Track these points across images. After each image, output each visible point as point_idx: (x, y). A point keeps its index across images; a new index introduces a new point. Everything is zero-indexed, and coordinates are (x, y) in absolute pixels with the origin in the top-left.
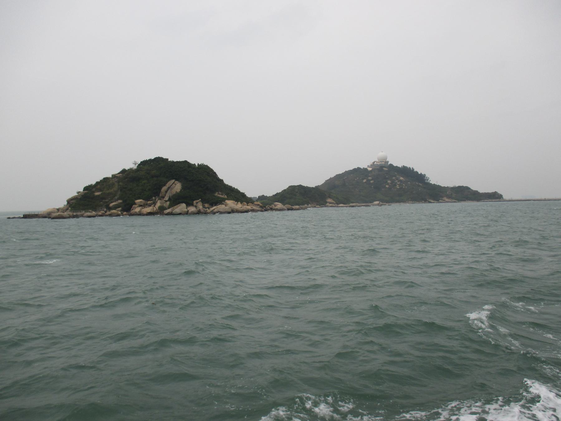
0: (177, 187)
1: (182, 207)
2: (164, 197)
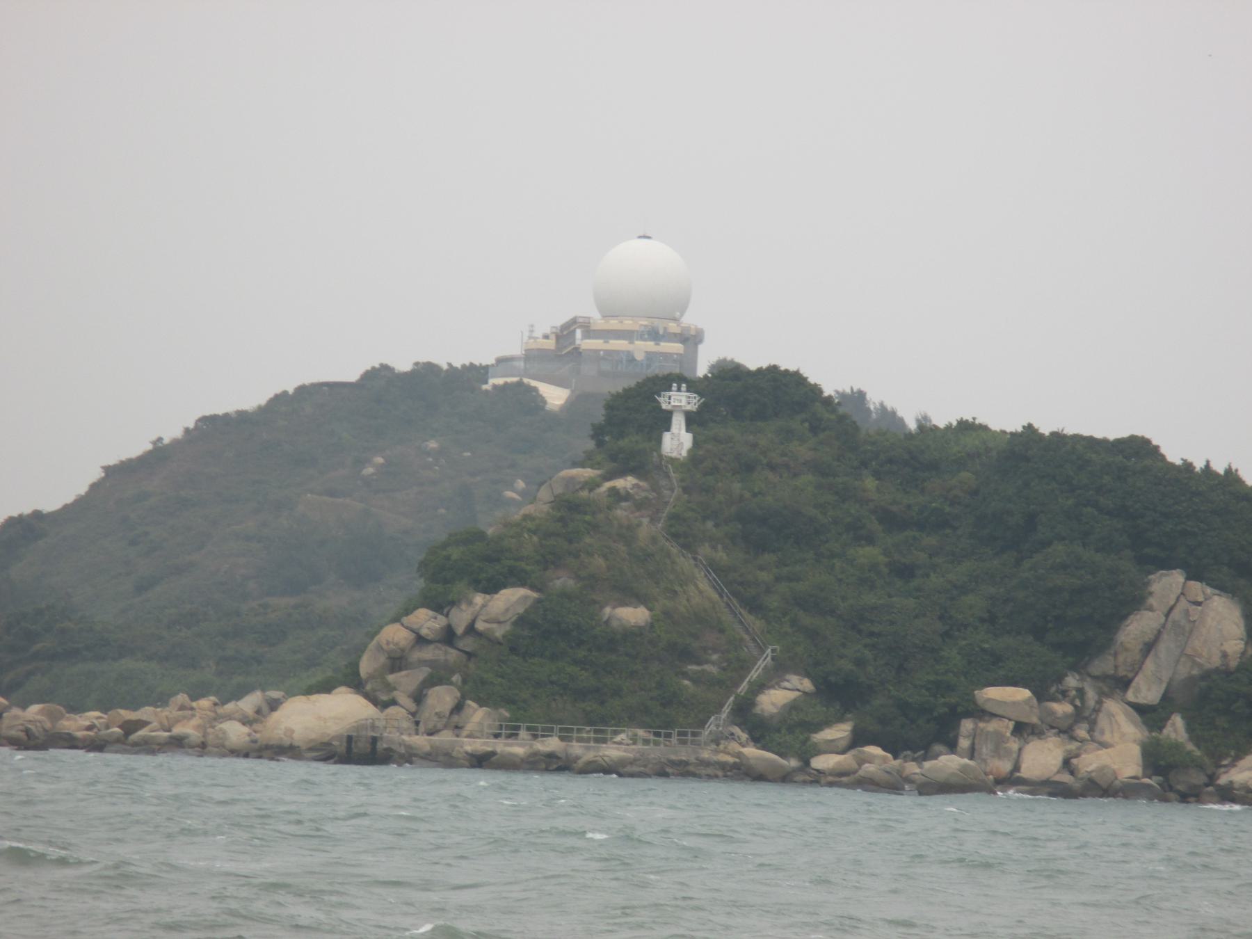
2: (1124, 684)
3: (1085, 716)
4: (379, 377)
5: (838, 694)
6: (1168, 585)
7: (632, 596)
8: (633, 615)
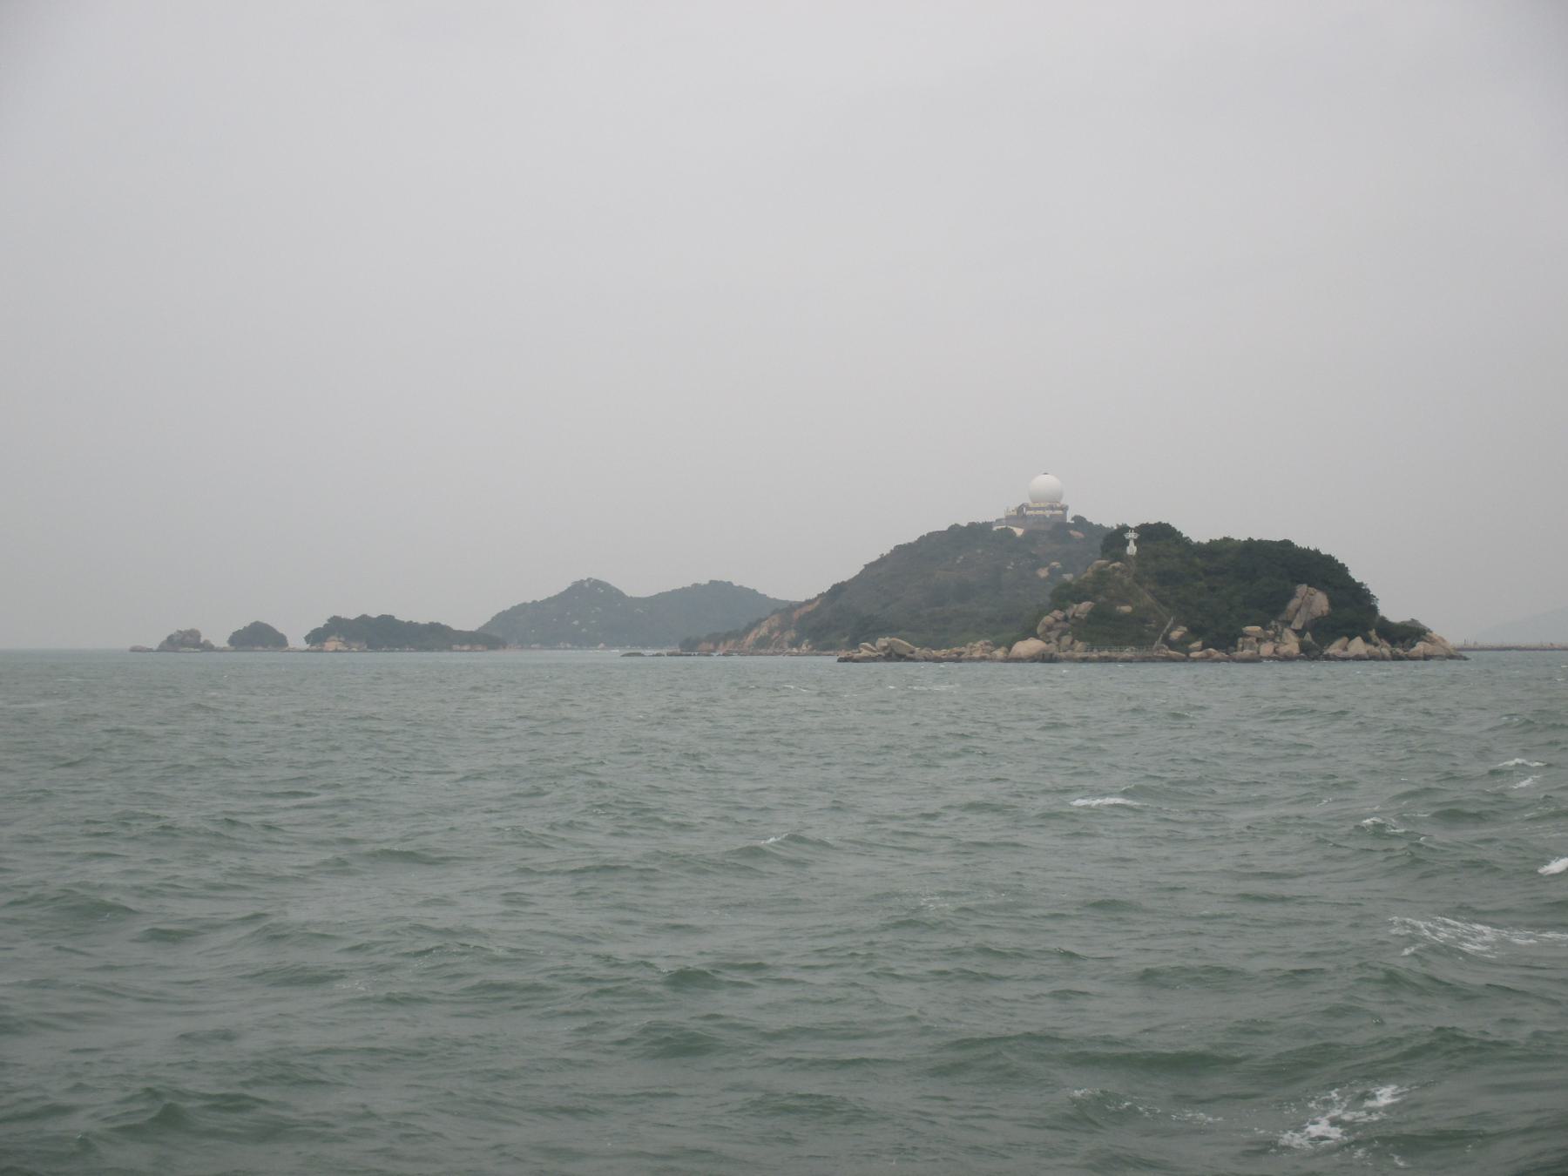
0: (1320, 602)
1: (1358, 646)
3: (1278, 634)
4: (955, 529)
5: (1196, 632)
6: (1302, 589)
7: (1125, 603)
8: (1127, 609)
